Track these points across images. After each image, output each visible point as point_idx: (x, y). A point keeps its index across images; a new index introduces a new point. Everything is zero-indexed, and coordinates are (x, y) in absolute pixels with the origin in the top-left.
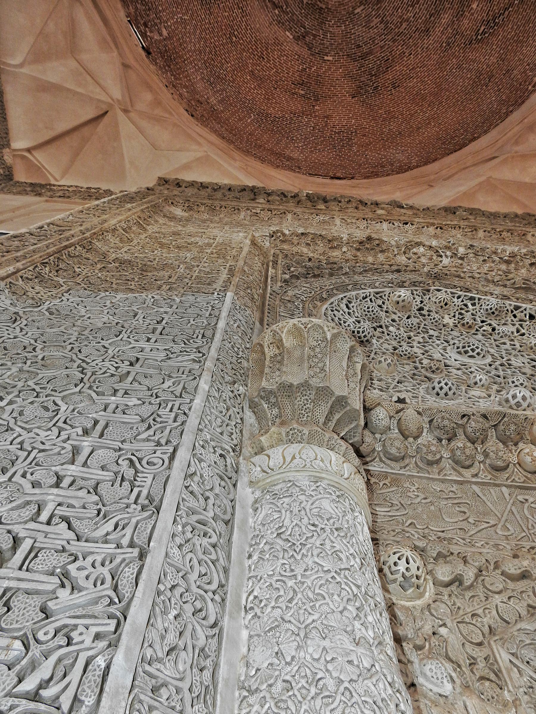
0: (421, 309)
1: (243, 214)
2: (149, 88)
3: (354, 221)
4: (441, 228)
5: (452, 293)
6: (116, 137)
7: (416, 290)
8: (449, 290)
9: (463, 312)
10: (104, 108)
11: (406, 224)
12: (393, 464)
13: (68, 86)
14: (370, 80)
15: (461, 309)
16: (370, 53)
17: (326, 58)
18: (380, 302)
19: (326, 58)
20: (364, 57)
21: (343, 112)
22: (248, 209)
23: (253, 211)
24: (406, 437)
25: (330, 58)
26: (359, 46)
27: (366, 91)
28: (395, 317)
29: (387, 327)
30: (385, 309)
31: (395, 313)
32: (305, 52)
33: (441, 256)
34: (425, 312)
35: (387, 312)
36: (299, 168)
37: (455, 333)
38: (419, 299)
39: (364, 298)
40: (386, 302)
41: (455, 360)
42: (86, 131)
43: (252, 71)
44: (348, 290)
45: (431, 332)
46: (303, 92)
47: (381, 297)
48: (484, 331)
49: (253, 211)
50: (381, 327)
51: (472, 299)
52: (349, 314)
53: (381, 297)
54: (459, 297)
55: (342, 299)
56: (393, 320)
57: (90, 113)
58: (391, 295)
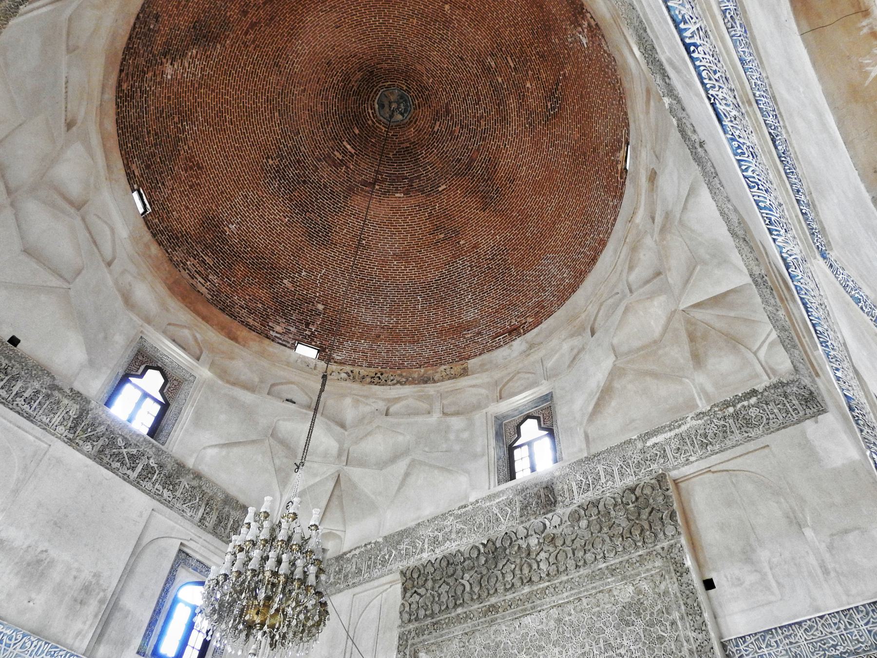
2: (343, 396)
6: (354, 486)
10: (337, 475)
13: (311, 482)
14: (486, 185)
16: (472, 160)
17: (440, 189)
19: (440, 189)
20: (469, 165)
21: (484, 235)
25: (444, 187)
26: (459, 160)
27: (491, 198)
32: (421, 198)
36: (479, 333)
42: (336, 493)
43: (394, 254)
46: (442, 236)
57: (331, 485)
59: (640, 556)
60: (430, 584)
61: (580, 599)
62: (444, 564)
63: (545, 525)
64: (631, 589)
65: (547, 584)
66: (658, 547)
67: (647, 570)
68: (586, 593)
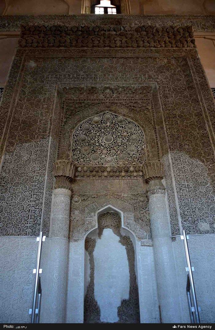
0: (102, 120)
1: (55, 60)
3: (95, 59)
4: (126, 59)
5: (111, 114)
7: (101, 114)
8: (111, 112)
9: (113, 120)
11: (113, 58)
12: (82, 177)
15: (113, 119)
18: (90, 122)
22: (57, 58)
23: (59, 59)
24: (84, 172)
28: (94, 126)
29: (91, 130)
30: (91, 124)
31: (94, 124)
33: (114, 93)
34: (102, 122)
35: (92, 125)
37: (108, 130)
38: (102, 117)
39: (85, 122)
40: (92, 121)
41: (104, 142)
44: (81, 121)
45: (103, 130)
47: (91, 120)
48: (116, 127)
49: (59, 59)
50: (89, 131)
51: (116, 116)
52: (81, 130)
53: (91, 120)
54: (113, 115)
55: (79, 126)
56: (93, 128)
58: (94, 119)
59: (174, 50)
60: (42, 35)
61: (138, 58)
62: (54, 29)
63: (121, 29)
64: (166, 61)
65: (120, 49)
66: (184, 49)
67: (178, 55)
68: (142, 56)
